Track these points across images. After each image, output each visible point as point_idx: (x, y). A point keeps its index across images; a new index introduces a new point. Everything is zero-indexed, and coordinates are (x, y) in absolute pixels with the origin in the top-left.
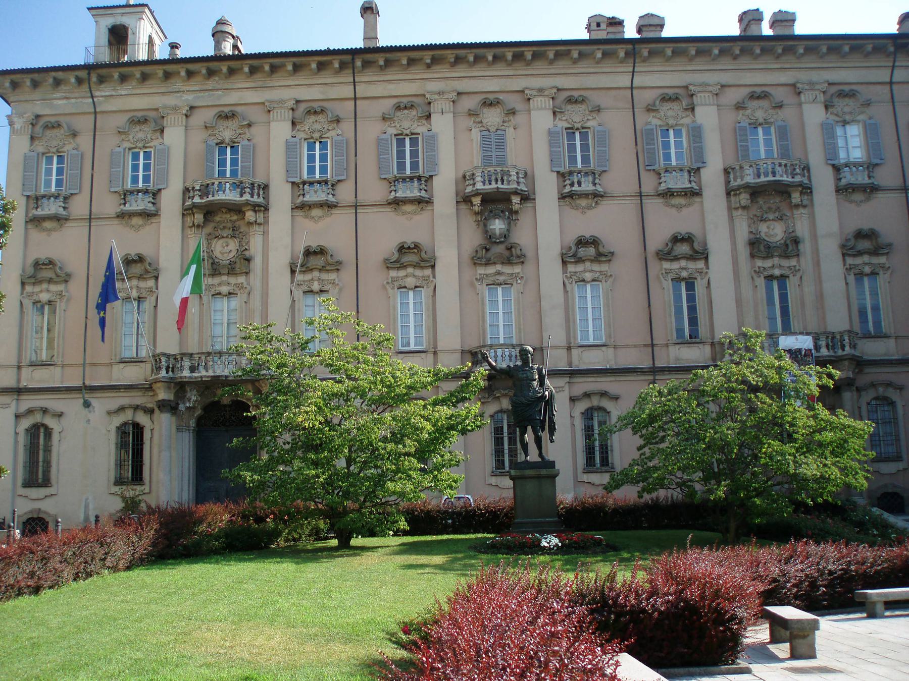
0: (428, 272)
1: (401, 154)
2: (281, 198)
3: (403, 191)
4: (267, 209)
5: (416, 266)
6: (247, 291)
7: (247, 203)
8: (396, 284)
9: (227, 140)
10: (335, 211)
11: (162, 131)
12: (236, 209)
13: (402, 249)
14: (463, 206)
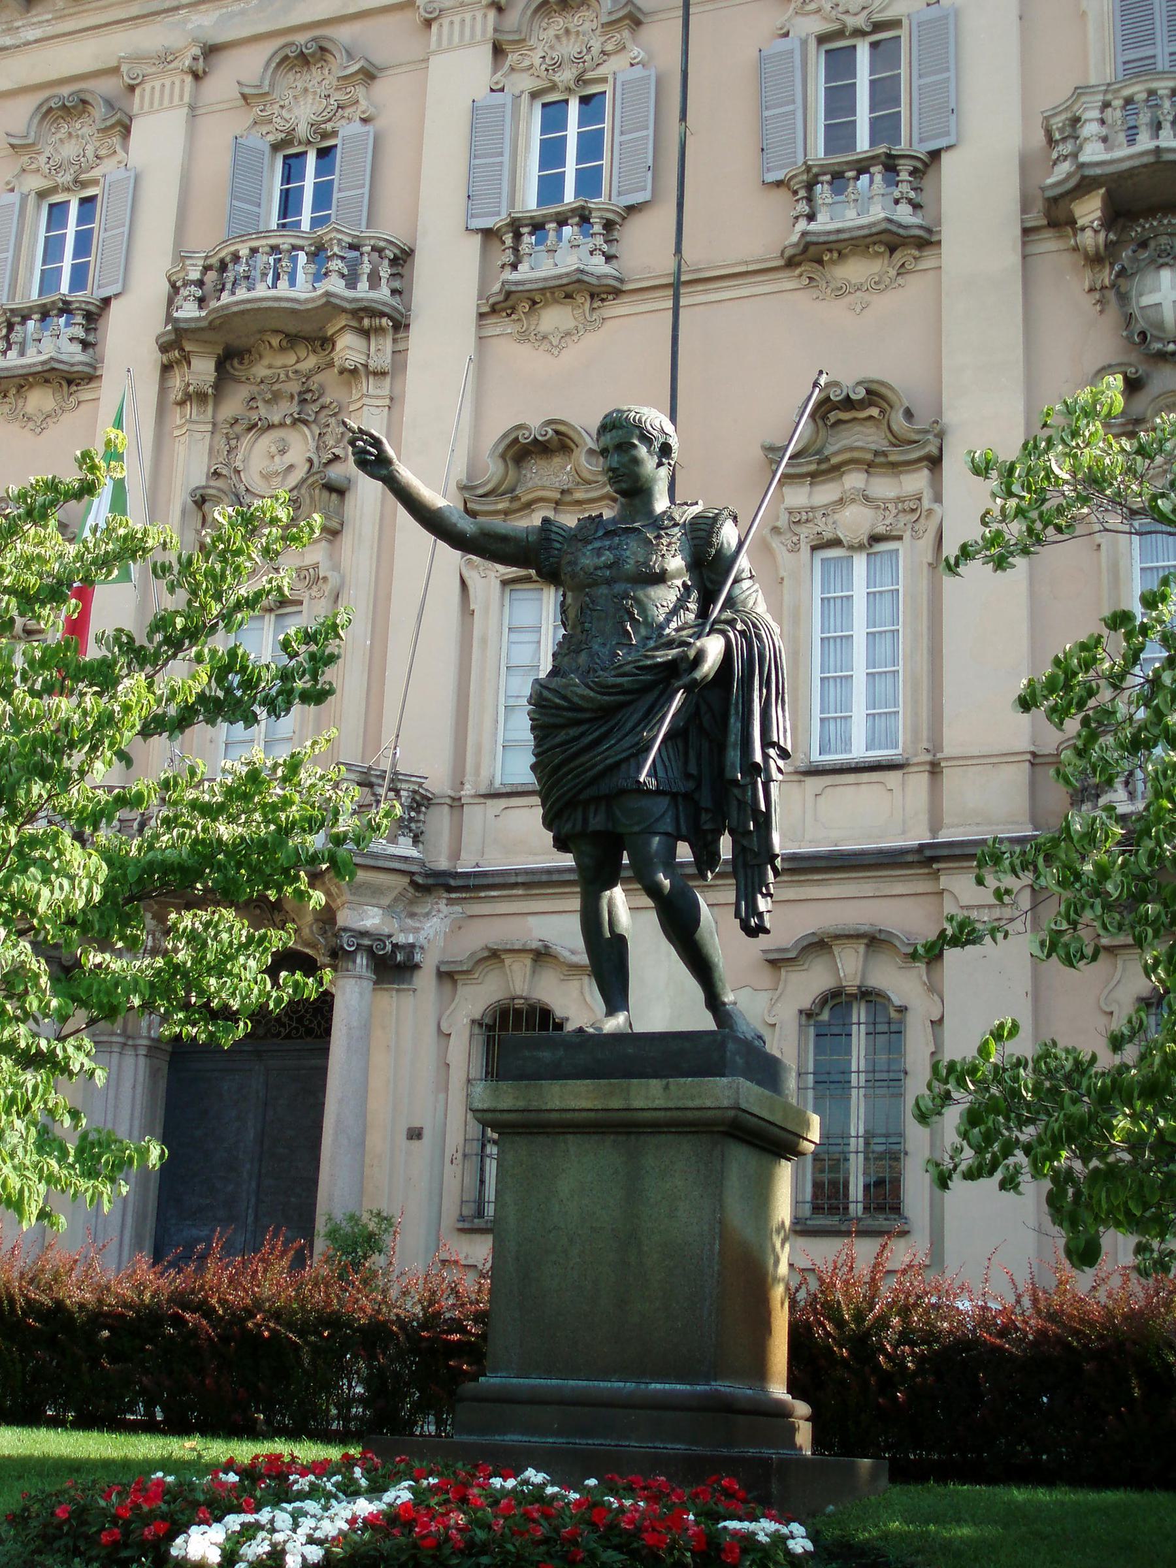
0: (917, 482)
1: (840, 100)
2: (448, 281)
3: (838, 216)
4: (400, 325)
5: (874, 464)
6: (327, 588)
7: (330, 307)
8: (805, 531)
9: (303, 131)
10: (616, 308)
11: (126, 130)
12: (308, 331)
13: (832, 410)
14: (1049, 244)
